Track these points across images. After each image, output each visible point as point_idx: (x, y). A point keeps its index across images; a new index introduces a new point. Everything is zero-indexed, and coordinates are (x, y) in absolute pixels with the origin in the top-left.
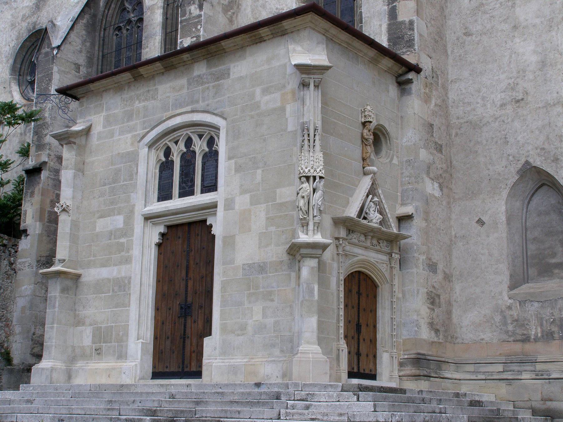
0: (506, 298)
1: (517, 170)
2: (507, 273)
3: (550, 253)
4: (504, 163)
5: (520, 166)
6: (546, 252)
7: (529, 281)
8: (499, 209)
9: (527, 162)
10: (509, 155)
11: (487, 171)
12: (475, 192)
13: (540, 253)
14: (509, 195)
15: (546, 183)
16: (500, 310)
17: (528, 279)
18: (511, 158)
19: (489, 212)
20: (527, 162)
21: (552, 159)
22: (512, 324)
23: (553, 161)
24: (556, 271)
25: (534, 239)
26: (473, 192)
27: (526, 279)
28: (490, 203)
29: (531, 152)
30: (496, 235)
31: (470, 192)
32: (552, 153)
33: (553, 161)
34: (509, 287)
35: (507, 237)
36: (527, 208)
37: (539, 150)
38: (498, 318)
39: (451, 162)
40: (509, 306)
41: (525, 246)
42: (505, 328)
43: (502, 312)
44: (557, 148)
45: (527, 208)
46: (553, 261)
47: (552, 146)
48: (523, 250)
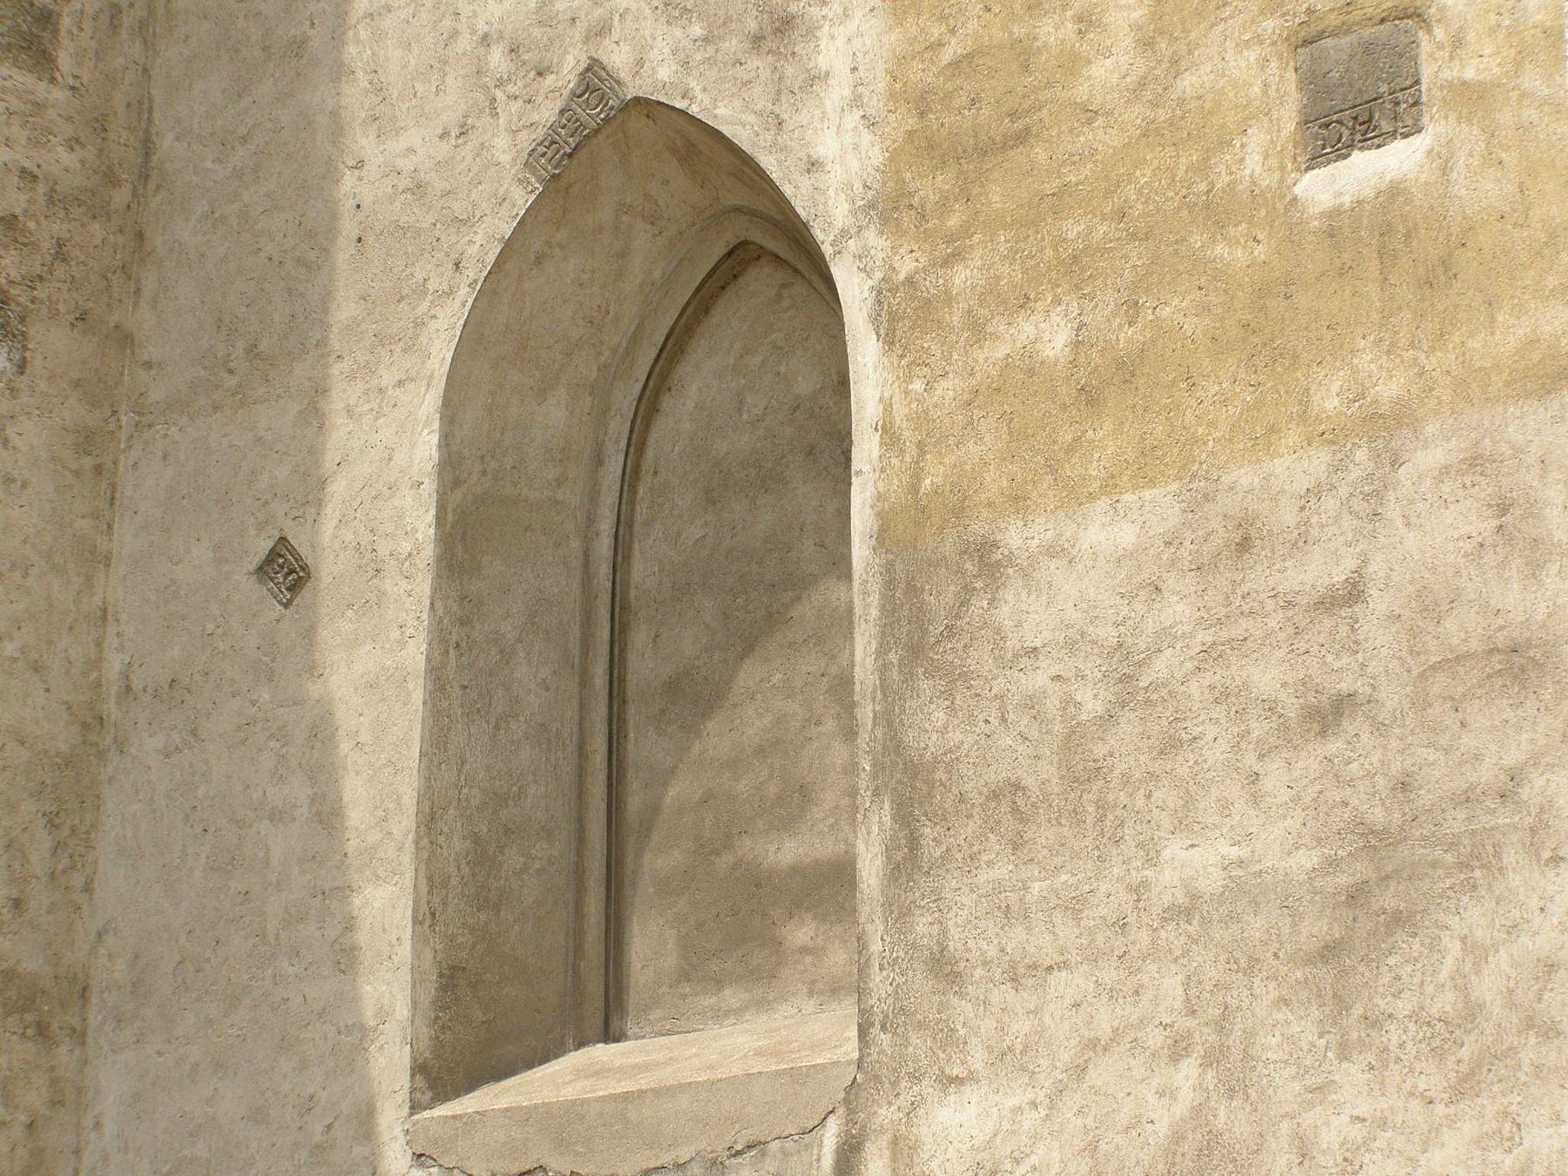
1: (527, 140)
3: (772, 789)
4: (452, 102)
5: (547, 113)
8: (400, 458)
9: (594, 80)
10: (485, 40)
12: (263, 346)
18: (497, 58)
20: (594, 80)
21: (752, 25)
26: (252, 349)
27: (594, 1006)
33: (757, 40)
39: (148, 147)
41: (599, 745)
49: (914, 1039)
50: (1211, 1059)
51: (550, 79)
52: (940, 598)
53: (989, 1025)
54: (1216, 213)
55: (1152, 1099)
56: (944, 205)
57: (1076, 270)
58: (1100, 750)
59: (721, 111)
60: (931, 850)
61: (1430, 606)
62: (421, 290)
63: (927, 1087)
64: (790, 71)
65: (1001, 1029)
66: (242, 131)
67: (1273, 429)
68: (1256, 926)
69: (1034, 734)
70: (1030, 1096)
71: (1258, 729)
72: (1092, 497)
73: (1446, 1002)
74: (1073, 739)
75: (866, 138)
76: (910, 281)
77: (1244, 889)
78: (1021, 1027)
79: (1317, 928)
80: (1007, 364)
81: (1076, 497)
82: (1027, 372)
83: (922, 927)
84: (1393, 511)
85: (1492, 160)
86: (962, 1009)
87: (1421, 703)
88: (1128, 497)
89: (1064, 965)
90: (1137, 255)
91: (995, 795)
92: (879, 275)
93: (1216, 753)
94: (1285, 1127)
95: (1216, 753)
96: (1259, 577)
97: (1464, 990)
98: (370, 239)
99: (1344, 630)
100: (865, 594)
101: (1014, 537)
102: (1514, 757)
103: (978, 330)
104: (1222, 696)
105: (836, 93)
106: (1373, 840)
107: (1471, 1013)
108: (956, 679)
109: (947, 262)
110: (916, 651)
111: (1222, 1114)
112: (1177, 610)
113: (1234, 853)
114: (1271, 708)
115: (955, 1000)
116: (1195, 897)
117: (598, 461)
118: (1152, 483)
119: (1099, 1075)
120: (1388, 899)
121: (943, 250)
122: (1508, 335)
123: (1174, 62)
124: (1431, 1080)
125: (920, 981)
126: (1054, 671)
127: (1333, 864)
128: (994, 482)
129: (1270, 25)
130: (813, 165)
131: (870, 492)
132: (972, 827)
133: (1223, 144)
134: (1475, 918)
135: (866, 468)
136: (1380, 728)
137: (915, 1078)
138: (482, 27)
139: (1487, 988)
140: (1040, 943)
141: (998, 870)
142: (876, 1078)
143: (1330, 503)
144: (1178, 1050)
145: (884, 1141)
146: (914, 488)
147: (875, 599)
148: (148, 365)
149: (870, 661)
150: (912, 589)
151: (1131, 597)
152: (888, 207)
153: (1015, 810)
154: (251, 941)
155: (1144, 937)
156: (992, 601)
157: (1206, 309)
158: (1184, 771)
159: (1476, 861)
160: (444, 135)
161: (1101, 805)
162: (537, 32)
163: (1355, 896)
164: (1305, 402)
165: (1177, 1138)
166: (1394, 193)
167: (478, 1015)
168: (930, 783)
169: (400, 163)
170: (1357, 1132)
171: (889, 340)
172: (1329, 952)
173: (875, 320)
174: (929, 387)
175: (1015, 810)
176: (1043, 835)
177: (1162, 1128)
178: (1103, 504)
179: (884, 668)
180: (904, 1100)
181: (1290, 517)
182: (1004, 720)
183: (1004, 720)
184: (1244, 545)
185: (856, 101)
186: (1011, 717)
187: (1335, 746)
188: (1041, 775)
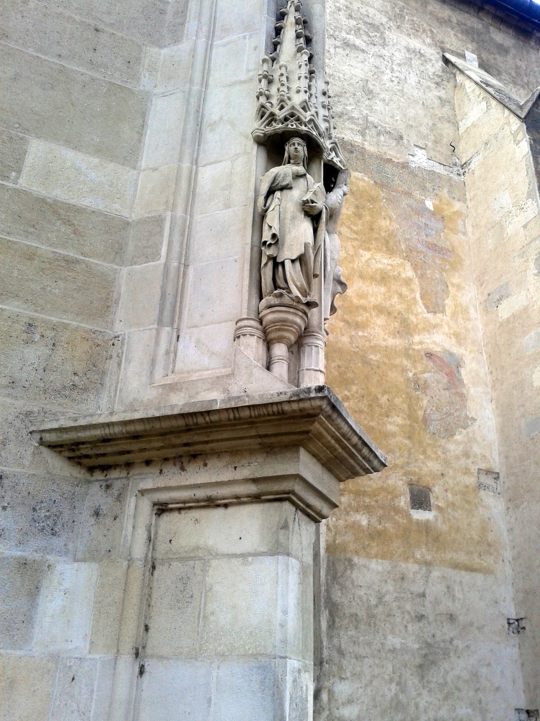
49: (333, 666)
50: (399, 684)
52: (340, 568)
53: (351, 667)
54: (397, 510)
55: (386, 690)
57: (368, 509)
58: (375, 612)
60: (337, 624)
61: (437, 602)
63: (337, 679)
65: (354, 668)
67: (408, 558)
68: (406, 657)
69: (360, 604)
70: (360, 685)
71: (407, 616)
72: (372, 558)
73: (441, 681)
74: (369, 608)
77: (404, 649)
78: (358, 669)
79: (418, 661)
80: (354, 523)
81: (369, 556)
82: (355, 526)
83: (335, 641)
84: (430, 581)
85: (444, 522)
86: (345, 663)
87: (436, 621)
88: (379, 560)
89: (367, 657)
90: (380, 512)
91: (352, 615)
93: (398, 620)
94: (413, 701)
95: (398, 620)
96: (405, 585)
97: (445, 679)
99: (422, 602)
100: (323, 561)
101: (356, 560)
102: (452, 635)
103: (348, 513)
104: (399, 608)
106: (429, 645)
107: (446, 683)
108: (343, 587)
110: (334, 578)
111: (401, 696)
112: (390, 587)
113: (403, 641)
114: (409, 613)
115: (343, 660)
116: (395, 649)
118: (384, 559)
119: (375, 683)
120: (431, 657)
122: (449, 555)
123: (387, 476)
124: (440, 696)
125: (335, 654)
126: (365, 592)
127: (421, 648)
128: (352, 547)
129: (404, 478)
131: (324, 539)
132: (346, 621)
133: (396, 497)
134: (446, 665)
135: (323, 533)
136: (429, 623)
137: (334, 676)
139: (449, 679)
140: (361, 651)
141: (352, 632)
142: (325, 675)
143: (419, 576)
144: (391, 680)
145: (326, 690)
146: (334, 541)
147: (325, 563)
149: (324, 577)
150: (333, 563)
151: (381, 581)
153: (356, 620)
155: (384, 655)
156: (351, 572)
157: (395, 528)
158: (392, 621)
159: (446, 654)
161: (374, 623)
163: (425, 656)
164: (413, 554)
165: (392, 700)
166: (428, 521)
168: (338, 609)
170: (426, 705)
172: (421, 666)
174: (336, 520)
175: (356, 620)
176: (362, 627)
177: (389, 697)
178: (374, 560)
179: (327, 579)
180: (331, 681)
181: (411, 575)
182: (354, 599)
183: (354, 599)
184: (403, 579)
186: (356, 599)
187: (421, 624)
188: (362, 614)
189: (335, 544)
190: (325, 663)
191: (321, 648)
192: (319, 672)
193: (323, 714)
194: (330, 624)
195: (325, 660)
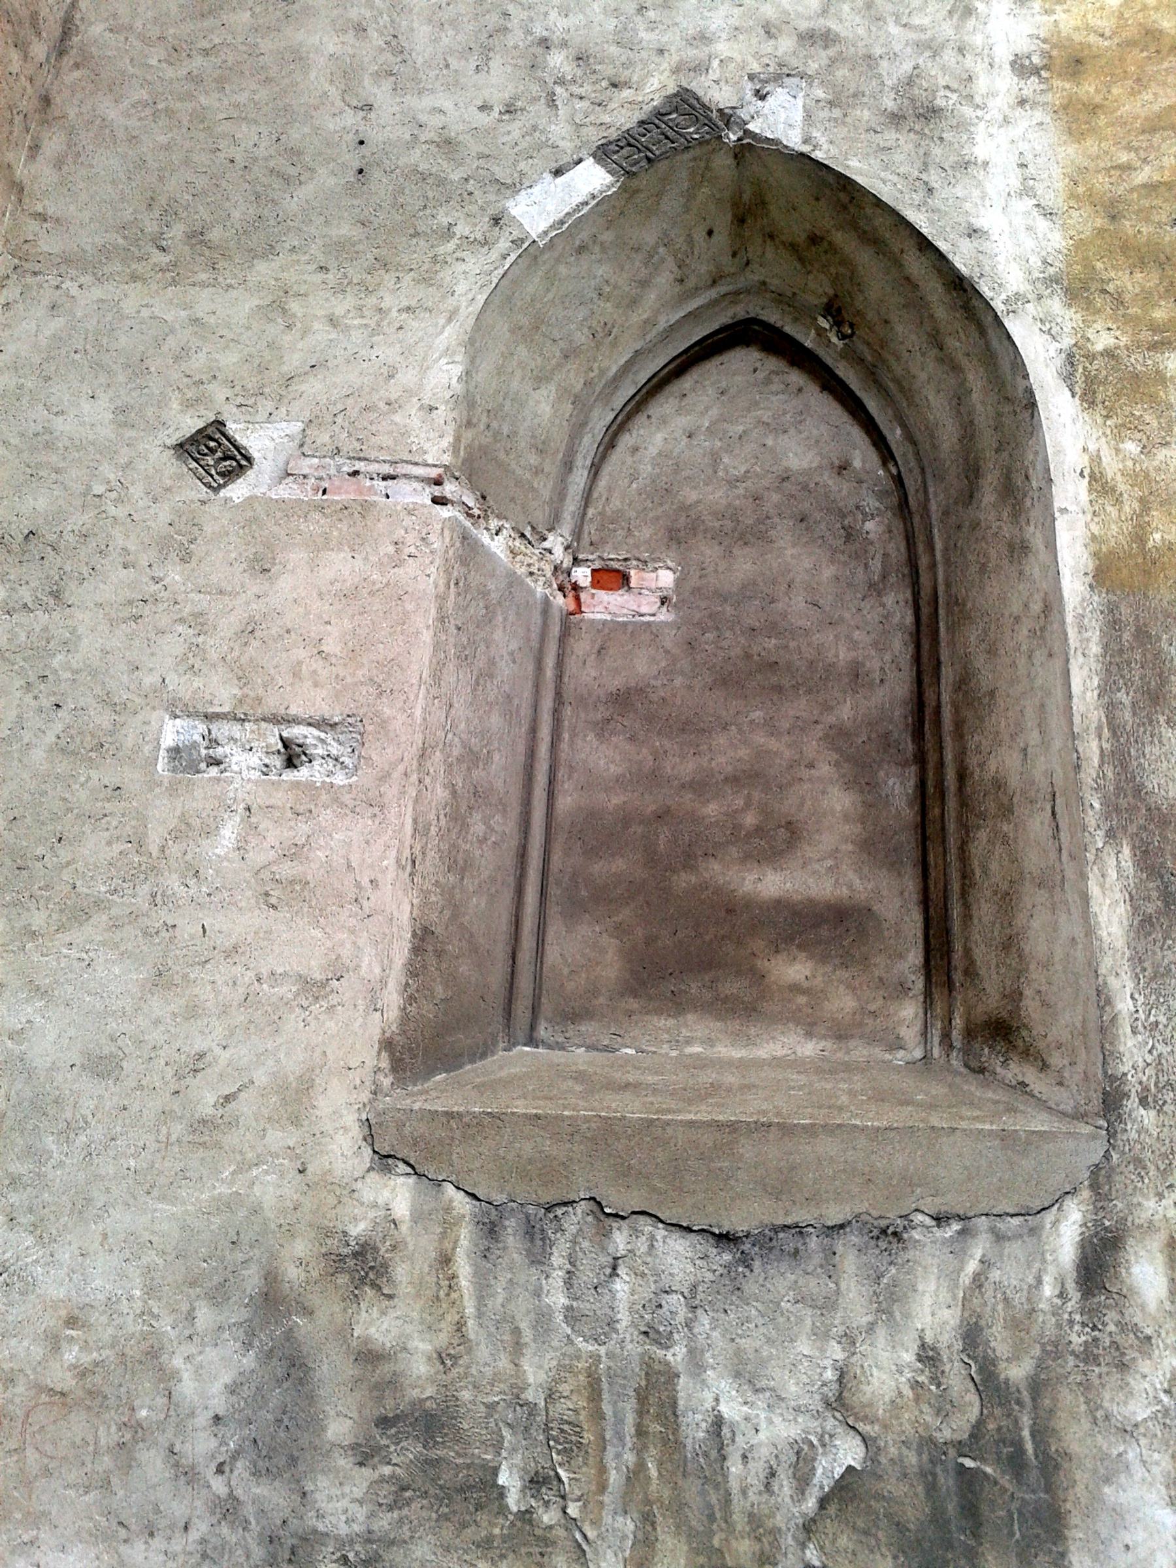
0: (344, 1151)
2: (398, 907)
3: (750, 820)
4: (499, 81)
5: (622, 116)
6: (712, 810)
7: (542, 1032)
8: (406, 377)
9: (685, 103)
11: (351, 119)
13: (660, 816)
14: (503, 296)
15: (772, 316)
16: (252, 1280)
17: (535, 1010)
19: (313, 387)
20: (685, 103)
21: (889, 103)
22: (365, 1455)
23: (896, 119)
24: (794, 969)
25: (623, 700)
26: (197, 236)
28: (332, 321)
29: (722, 48)
30: (340, 566)
31: (178, 231)
32: (893, 73)
33: (896, 119)
34: (387, 1045)
35: (441, 598)
36: (595, 470)
37: (786, 44)
38: (211, 1372)
40: (364, 1251)
41: (545, 732)
42: (271, 1496)
43: (272, 1301)
44: (933, 48)
45: (595, 470)
46: (770, 883)
47: (894, 29)
48: (531, 753)
51: (626, 93)
56: (1147, 298)
59: (854, 163)
62: (448, 232)
64: (937, 151)
66: (205, 44)
75: (1042, 224)
76: (1109, 353)
92: (1067, 342)
98: (377, 174)
100: (1081, 628)
105: (1001, 178)
109: (1153, 347)
117: (568, 466)
121: (1146, 336)
130: (973, 232)
131: (1080, 531)
138: (539, 31)
142: (1138, 1162)
147: (1095, 636)
148: (42, 217)
149: (1092, 696)
150: (1142, 635)
152: (1079, 286)
154: (117, 847)
160: (484, 108)
162: (613, 50)
167: (440, 991)
169: (423, 118)
171: (1089, 399)
173: (1068, 378)
179: (1111, 709)
185: (1026, 191)
189: (1143, 550)
190: (1132, 1103)
191: (1102, 1030)
192: (1100, 1147)
193: (1145, 1366)
194: (1150, 909)
195: (1133, 1086)
